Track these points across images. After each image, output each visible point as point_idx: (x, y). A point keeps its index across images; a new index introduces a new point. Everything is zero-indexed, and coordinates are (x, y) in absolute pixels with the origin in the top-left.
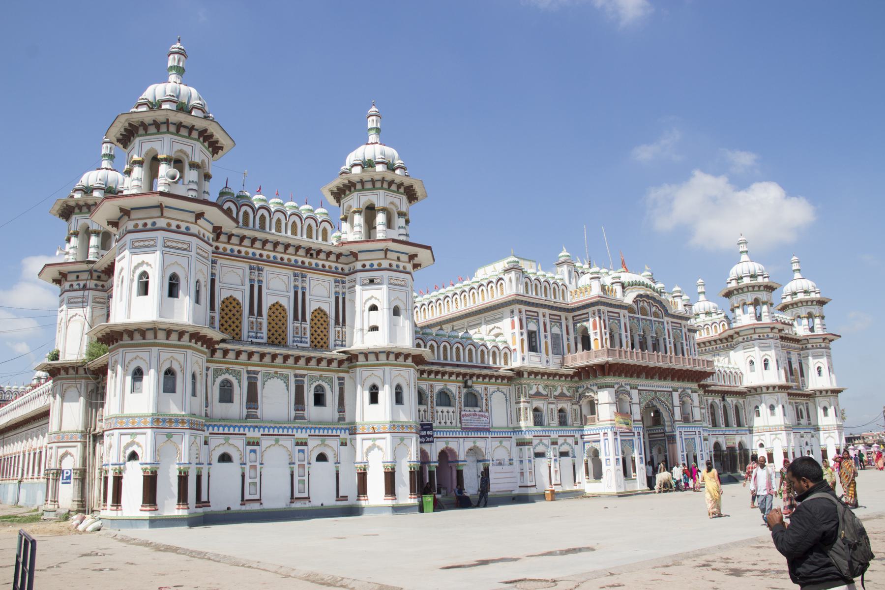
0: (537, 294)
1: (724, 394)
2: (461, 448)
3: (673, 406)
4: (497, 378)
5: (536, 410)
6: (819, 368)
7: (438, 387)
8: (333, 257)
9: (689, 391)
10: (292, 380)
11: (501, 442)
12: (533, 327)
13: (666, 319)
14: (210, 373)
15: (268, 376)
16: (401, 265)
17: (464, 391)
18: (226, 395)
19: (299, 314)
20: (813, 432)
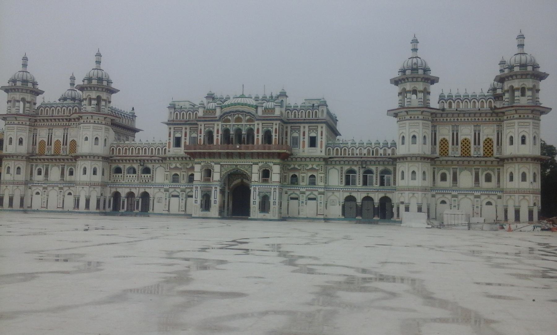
0: (183, 118)
1: (363, 162)
2: (137, 192)
3: (252, 173)
4: (158, 160)
5: (176, 175)
6: (511, 139)
7: (128, 166)
8: (76, 120)
9: (271, 164)
10: (61, 166)
11: (160, 190)
12: (178, 135)
13: (256, 123)
14: (34, 167)
15: (52, 166)
16: (88, 121)
17: (141, 167)
18: (40, 173)
19: (65, 143)
20: (499, 194)
